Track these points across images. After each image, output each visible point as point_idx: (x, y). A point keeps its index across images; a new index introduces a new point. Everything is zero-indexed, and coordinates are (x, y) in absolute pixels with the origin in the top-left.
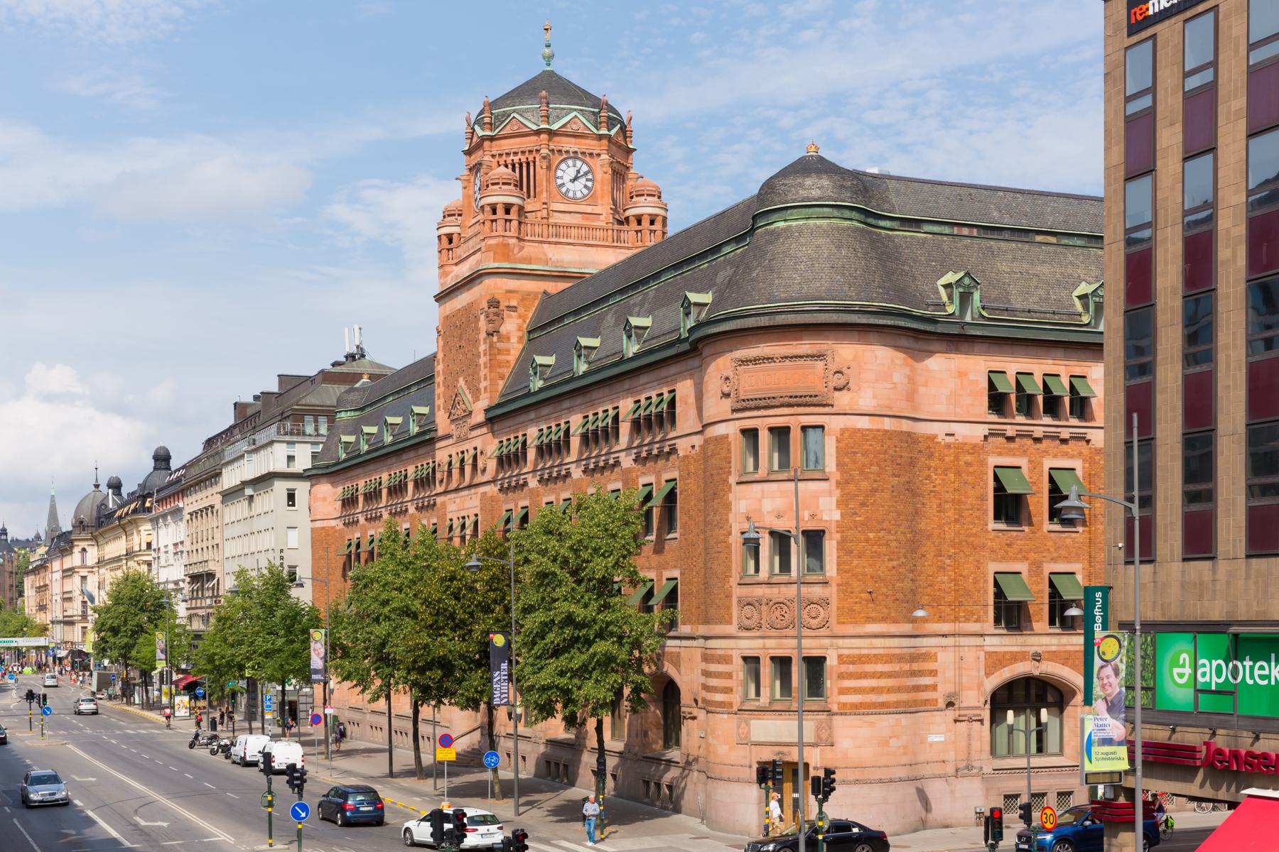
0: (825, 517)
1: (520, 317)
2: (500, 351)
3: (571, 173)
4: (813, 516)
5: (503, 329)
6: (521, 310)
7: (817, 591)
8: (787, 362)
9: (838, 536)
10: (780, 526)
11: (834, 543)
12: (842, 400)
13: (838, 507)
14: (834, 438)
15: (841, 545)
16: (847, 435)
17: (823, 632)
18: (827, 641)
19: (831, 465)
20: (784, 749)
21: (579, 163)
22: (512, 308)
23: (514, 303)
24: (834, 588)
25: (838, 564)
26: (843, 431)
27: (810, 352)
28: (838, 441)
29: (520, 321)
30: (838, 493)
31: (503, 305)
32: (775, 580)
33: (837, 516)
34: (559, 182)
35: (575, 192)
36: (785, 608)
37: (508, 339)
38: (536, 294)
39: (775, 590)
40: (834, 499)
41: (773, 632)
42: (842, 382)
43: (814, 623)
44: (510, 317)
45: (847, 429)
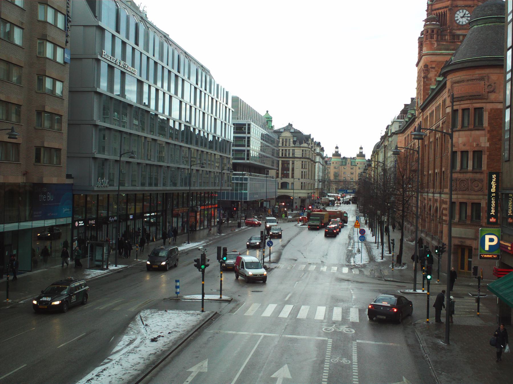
0: (483, 145)
1: (436, 71)
2: (427, 85)
3: (462, 14)
4: (477, 145)
5: (429, 76)
6: (437, 69)
7: (478, 176)
8: (470, 82)
9: (488, 153)
10: (464, 148)
11: (486, 156)
12: (492, 96)
13: (488, 141)
14: (487, 113)
15: (489, 157)
16: (493, 111)
17: (480, 193)
18: (481, 197)
19: (486, 124)
20: (463, 240)
21: (465, 11)
22: (432, 68)
23: (434, 66)
24: (485, 175)
25: (487, 165)
26: (491, 110)
27: (478, 78)
28: (489, 114)
29: (436, 73)
30: (488, 135)
31: (429, 67)
32: (475, 170)
33: (488, 145)
34: (456, 19)
35: (460, 22)
36: (465, 182)
37: (431, 80)
38: (443, 62)
39: (462, 175)
40: (487, 138)
41: (461, 192)
42: (492, 89)
43: (476, 189)
44: (432, 71)
45: (494, 109)
